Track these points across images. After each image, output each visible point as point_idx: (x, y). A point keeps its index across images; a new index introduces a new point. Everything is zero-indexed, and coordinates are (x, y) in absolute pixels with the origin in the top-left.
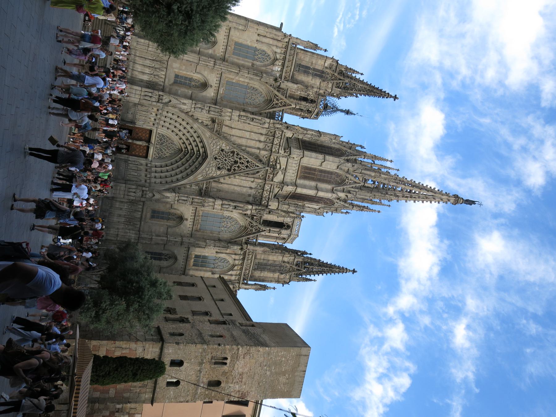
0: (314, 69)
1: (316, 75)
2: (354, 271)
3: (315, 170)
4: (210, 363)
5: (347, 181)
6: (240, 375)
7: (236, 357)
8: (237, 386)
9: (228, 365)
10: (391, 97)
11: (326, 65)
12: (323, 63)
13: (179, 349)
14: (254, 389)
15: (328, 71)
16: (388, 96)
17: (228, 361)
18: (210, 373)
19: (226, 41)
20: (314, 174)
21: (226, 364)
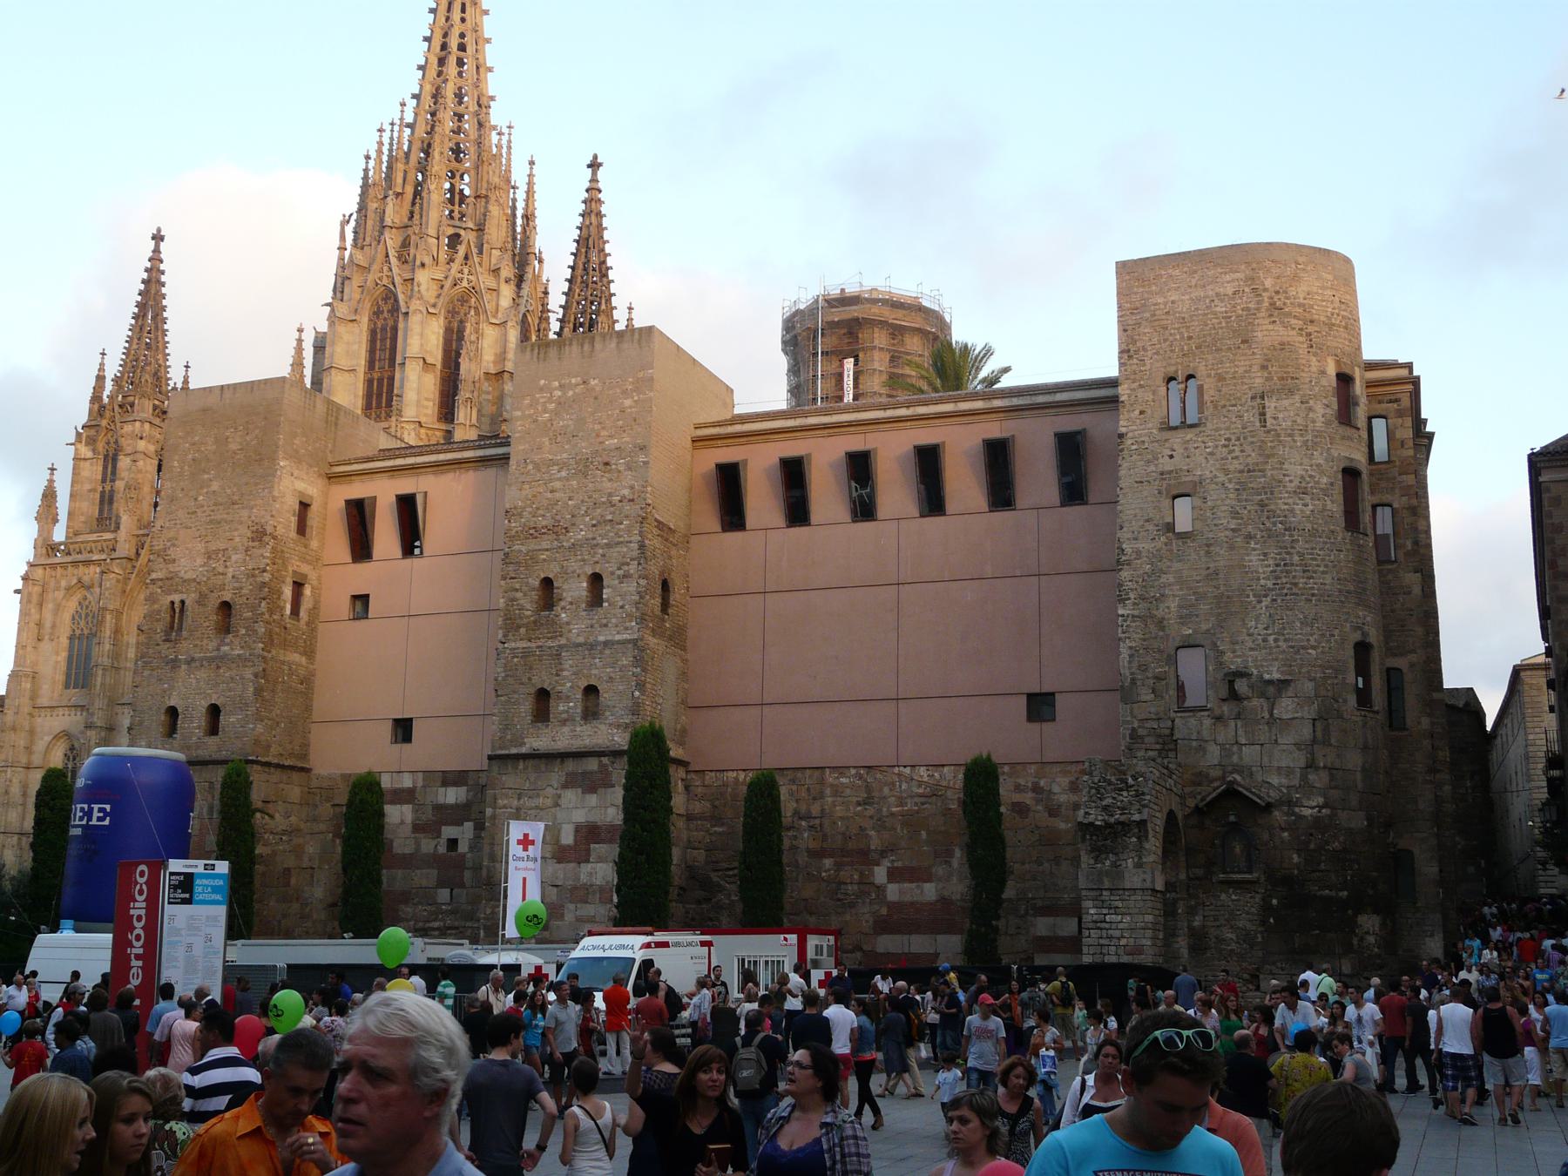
0: (104, 481)
1: (114, 473)
2: (594, 165)
3: (369, 382)
4: (176, 641)
5: (385, 281)
6: (209, 558)
7: (170, 582)
8: (234, 558)
9: (184, 597)
10: (157, 251)
11: (89, 454)
12: (88, 463)
13: (141, 723)
14: (245, 513)
15: (101, 446)
16: (156, 258)
17: (177, 598)
18: (201, 639)
19: (61, 711)
20: (380, 380)
21: (183, 602)
